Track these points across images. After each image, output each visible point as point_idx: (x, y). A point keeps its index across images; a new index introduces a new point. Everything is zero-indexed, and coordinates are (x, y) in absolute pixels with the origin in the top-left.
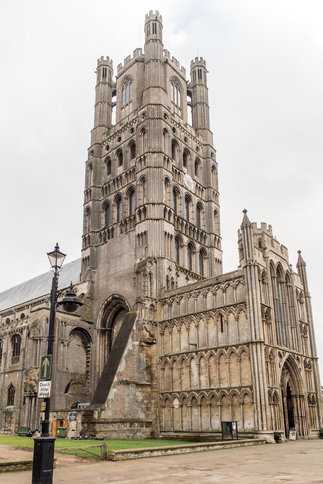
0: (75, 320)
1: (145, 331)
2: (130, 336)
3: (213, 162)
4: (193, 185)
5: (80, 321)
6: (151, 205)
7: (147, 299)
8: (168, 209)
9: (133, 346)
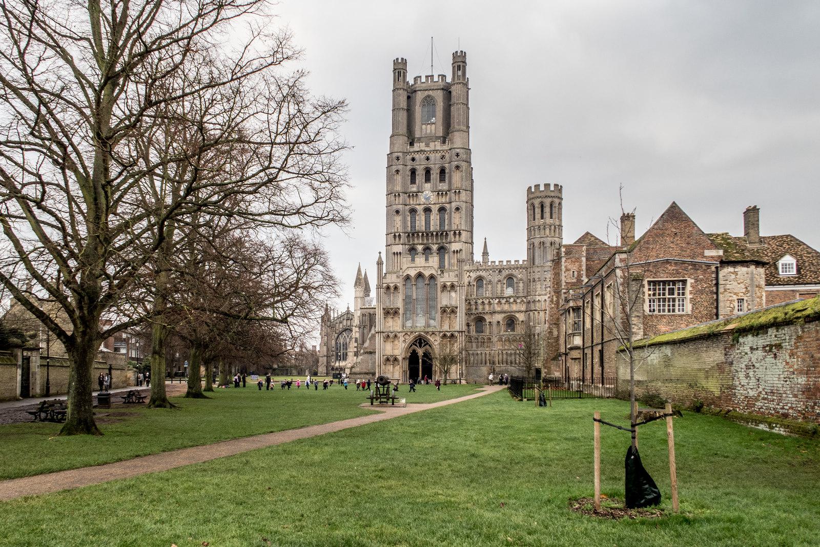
3: (456, 163)
8: (397, 234)
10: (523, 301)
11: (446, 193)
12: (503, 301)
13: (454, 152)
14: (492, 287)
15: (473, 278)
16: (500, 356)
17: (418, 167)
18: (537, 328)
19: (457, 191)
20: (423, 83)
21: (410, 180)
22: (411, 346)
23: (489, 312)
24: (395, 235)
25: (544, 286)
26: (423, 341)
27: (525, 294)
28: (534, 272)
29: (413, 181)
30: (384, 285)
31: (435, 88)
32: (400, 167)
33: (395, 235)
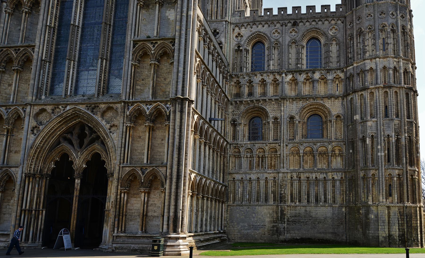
12: (302, 78)
14: (281, 54)
15: (245, 38)
16: (296, 184)
18: (369, 124)
23: (273, 98)
25: (381, 41)
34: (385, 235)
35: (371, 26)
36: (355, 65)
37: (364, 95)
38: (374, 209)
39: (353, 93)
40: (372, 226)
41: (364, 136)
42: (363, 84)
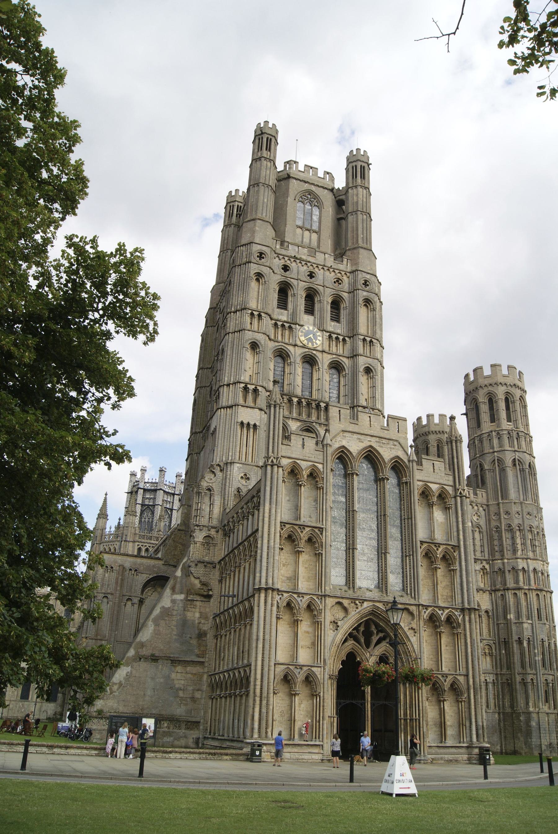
0: (153, 566)
1: (192, 579)
2: (169, 586)
3: (365, 293)
4: (320, 338)
5: (162, 567)
6: (225, 386)
7: (199, 528)
8: (251, 387)
9: (173, 601)
10: (484, 569)
11: (344, 340)
13: (361, 277)
17: (294, 282)
18: (525, 625)
19: (368, 339)
20: (299, 171)
21: (275, 303)
22: (346, 641)
24: (246, 389)
26: (373, 628)
27: (487, 558)
28: (507, 513)
29: (283, 303)
30: (285, 462)
31: (320, 185)
32: (265, 270)
33: (246, 389)
34: (546, 743)
35: (520, 524)
36: (506, 561)
37: (518, 594)
38: (534, 716)
39: (504, 590)
40: (535, 734)
41: (519, 638)
42: (517, 581)
